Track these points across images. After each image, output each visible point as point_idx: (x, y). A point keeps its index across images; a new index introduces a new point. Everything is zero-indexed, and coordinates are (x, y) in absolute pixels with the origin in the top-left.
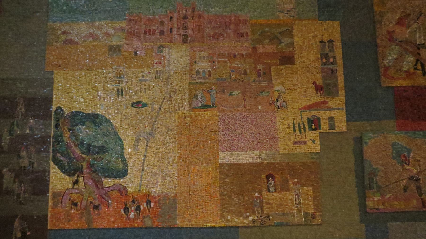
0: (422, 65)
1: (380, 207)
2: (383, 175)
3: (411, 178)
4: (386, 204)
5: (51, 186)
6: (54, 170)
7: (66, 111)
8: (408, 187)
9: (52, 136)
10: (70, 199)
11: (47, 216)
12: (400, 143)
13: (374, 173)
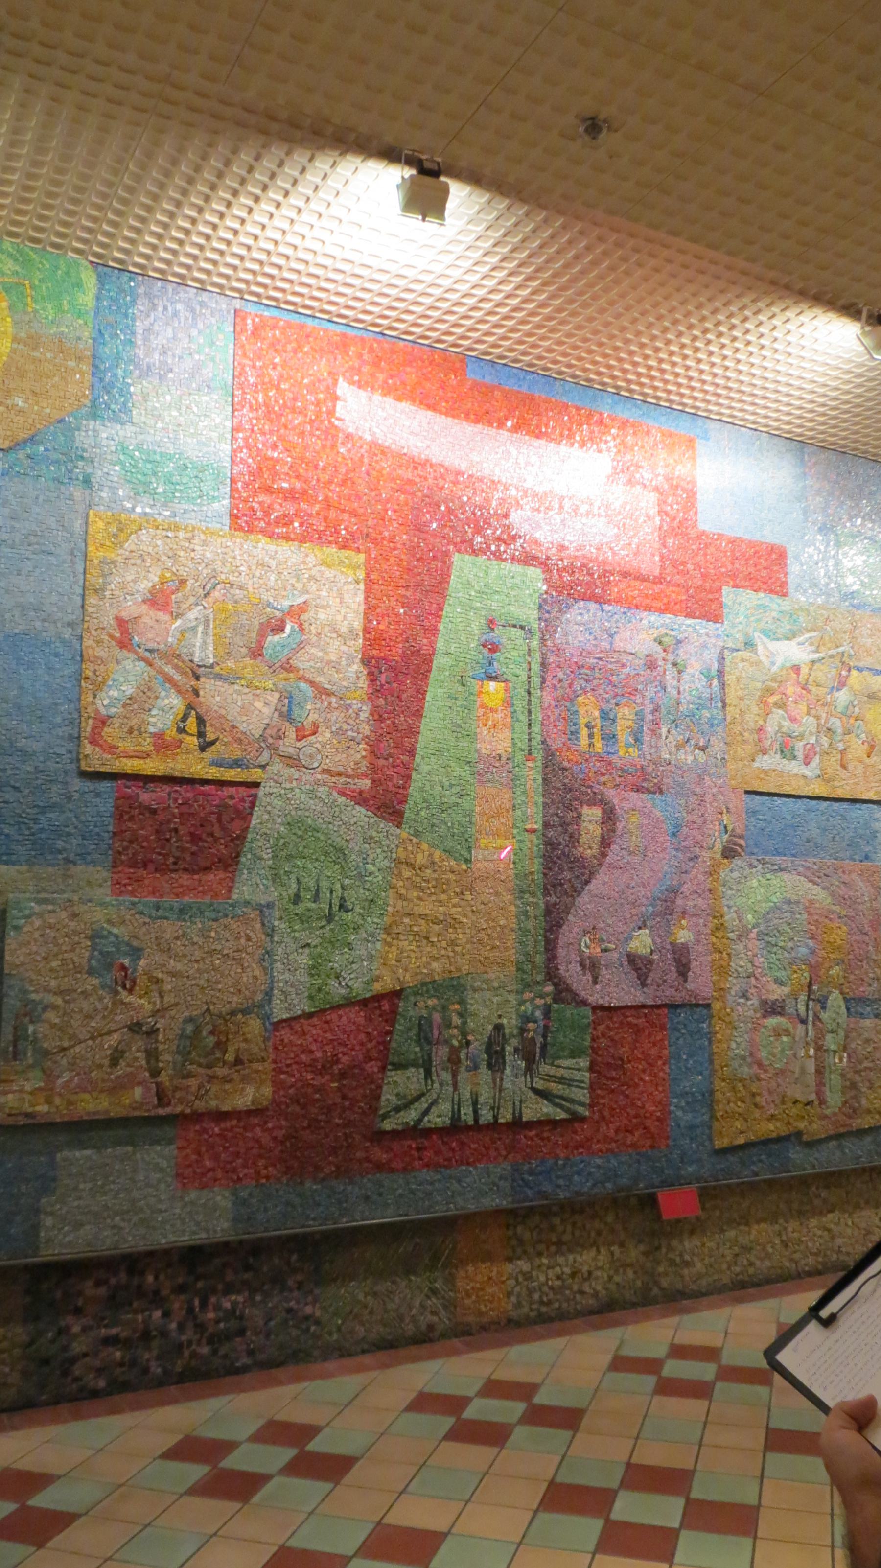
0: (201, 721)
1: (38, 1108)
2: (57, 1021)
3: (135, 1028)
4: (57, 1101)
8: (123, 1052)
12: (115, 931)
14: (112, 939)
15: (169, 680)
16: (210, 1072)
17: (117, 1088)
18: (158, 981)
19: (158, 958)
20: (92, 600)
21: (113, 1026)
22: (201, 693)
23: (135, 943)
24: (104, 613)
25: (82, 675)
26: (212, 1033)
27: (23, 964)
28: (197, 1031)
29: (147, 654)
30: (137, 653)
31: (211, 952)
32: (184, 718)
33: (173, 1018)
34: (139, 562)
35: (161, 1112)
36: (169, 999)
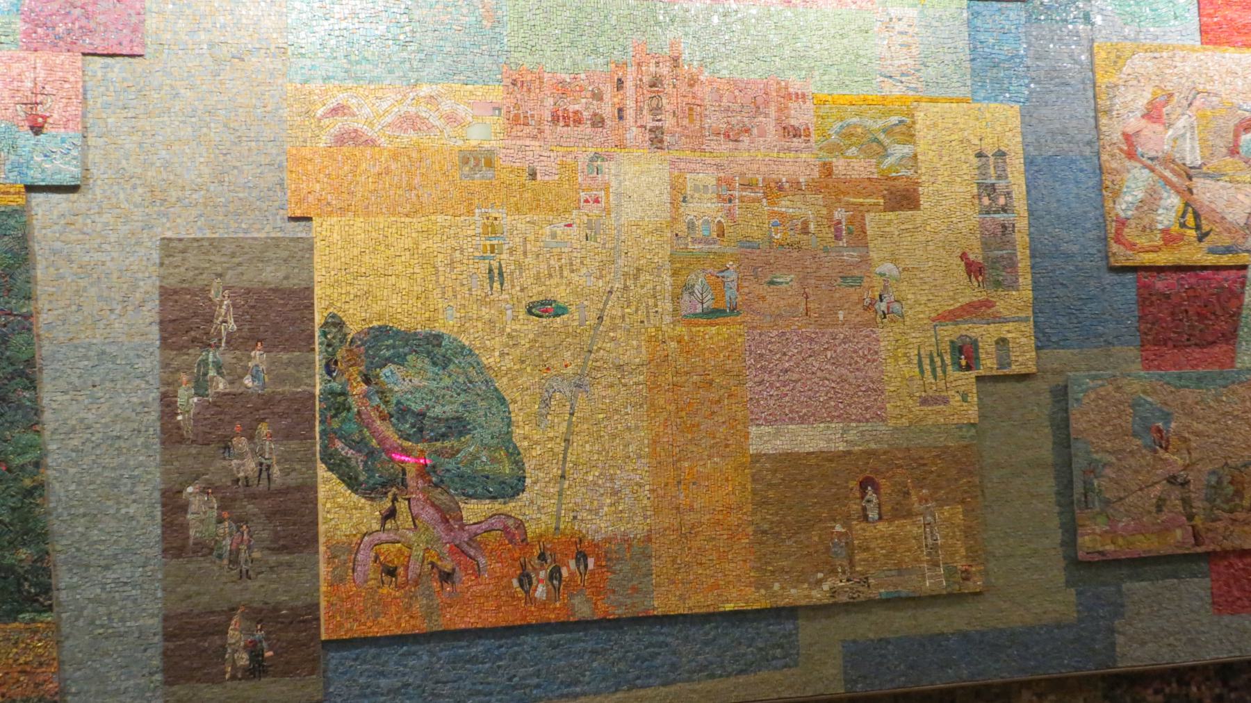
0: (1197, 216)
1: (1107, 548)
3: (1172, 480)
4: (1120, 541)
5: (322, 528)
6: (328, 486)
7: (353, 329)
8: (1165, 500)
9: (317, 393)
10: (377, 558)
11: (317, 605)
12: (1149, 399)
13: (1093, 469)
14: (1147, 406)
15: (1167, 182)
16: (1232, 516)
17: (1165, 529)
18: (1186, 440)
19: (1185, 420)
20: (1104, 120)
21: (1156, 479)
22: (1195, 191)
23: (1165, 409)
24: (1113, 130)
25: (1103, 184)
26: (1231, 483)
27: (1085, 430)
28: (1219, 482)
29: (1149, 162)
30: (1141, 162)
31: (1225, 414)
32: (1183, 216)
33: (1199, 471)
34: (1135, 82)
35: (1199, 550)
36: (1195, 455)
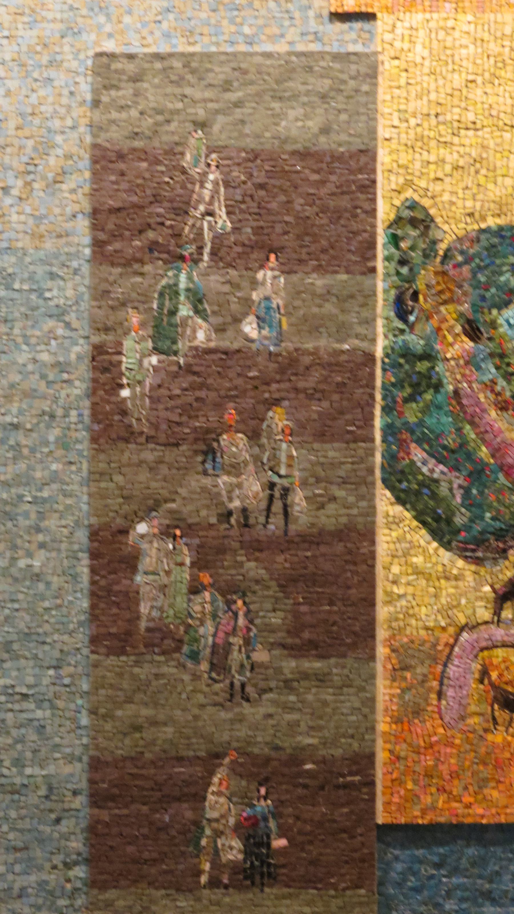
5: (382, 612)
7: (449, 231)
9: (379, 353)
10: (485, 673)
11: (371, 757)
